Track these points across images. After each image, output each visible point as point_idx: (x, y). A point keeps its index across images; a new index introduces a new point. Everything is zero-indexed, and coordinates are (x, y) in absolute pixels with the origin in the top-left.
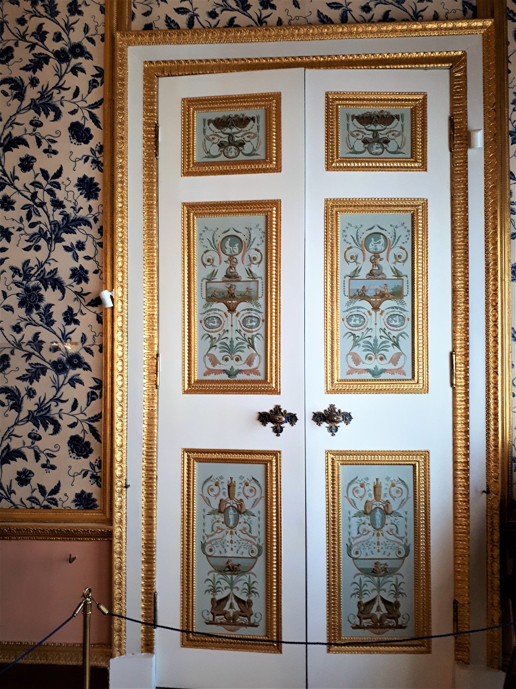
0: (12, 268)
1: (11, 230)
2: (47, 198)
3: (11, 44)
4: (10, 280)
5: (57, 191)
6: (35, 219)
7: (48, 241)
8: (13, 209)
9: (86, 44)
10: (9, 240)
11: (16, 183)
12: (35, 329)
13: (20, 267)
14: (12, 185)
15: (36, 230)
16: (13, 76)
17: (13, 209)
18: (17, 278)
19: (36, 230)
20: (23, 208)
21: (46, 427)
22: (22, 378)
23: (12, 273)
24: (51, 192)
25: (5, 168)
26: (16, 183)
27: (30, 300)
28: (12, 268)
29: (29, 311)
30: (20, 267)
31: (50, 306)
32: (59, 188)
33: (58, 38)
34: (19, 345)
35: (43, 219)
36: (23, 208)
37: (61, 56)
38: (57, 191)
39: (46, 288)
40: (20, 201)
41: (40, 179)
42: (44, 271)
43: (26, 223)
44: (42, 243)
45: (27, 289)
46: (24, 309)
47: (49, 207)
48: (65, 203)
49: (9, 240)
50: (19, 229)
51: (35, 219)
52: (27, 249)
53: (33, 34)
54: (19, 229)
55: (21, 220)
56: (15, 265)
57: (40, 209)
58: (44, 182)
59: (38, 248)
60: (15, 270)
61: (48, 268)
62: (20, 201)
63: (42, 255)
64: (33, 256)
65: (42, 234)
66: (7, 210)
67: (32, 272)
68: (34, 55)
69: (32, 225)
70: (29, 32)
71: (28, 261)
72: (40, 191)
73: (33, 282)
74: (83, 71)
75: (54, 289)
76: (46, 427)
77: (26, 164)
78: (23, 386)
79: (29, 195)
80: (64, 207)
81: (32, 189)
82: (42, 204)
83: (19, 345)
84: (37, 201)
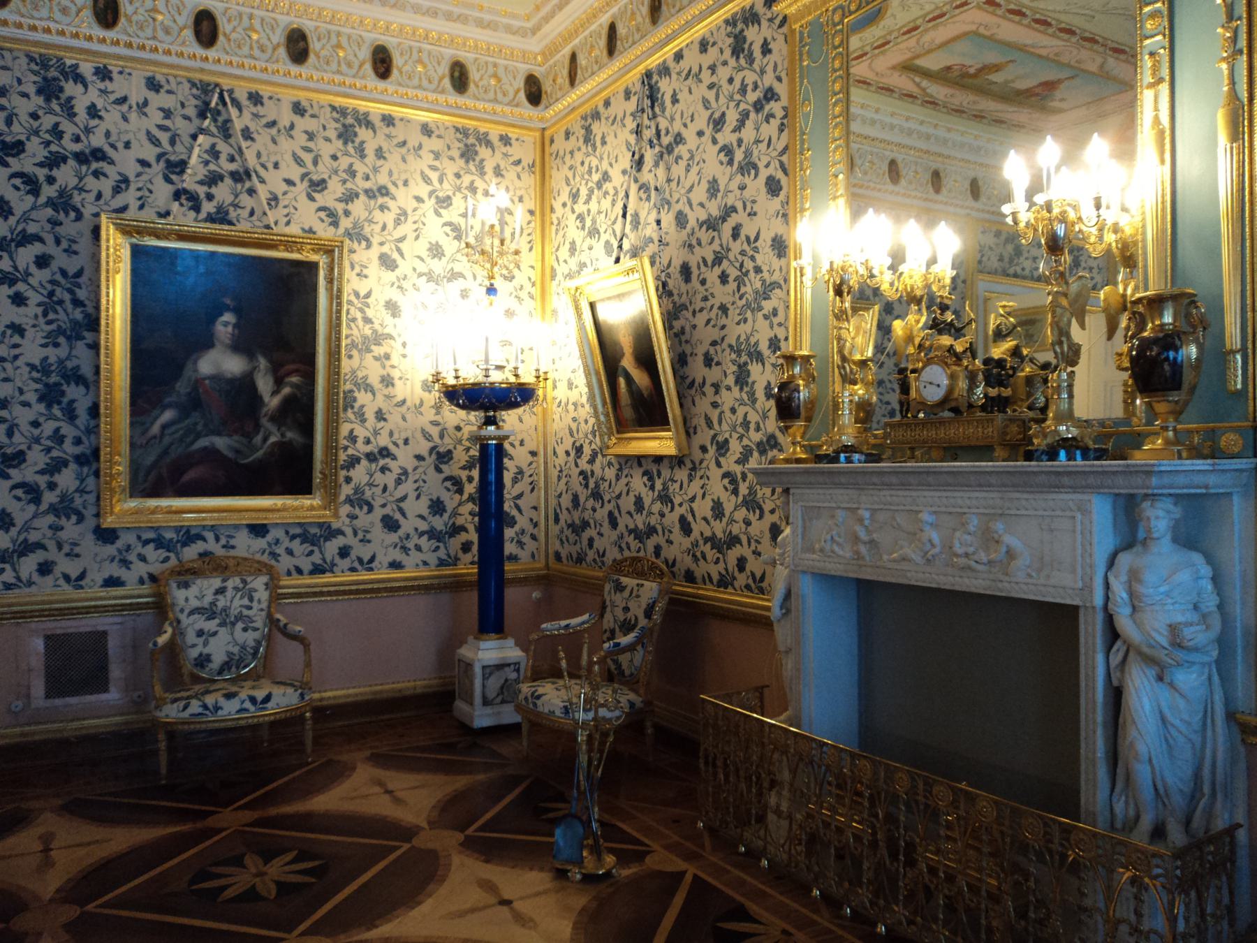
0: (28, 365)
1: (26, 327)
2: (67, 297)
3: (23, 138)
4: (26, 376)
5: (77, 290)
6: (51, 316)
7: (69, 338)
8: (26, 305)
9: (107, 149)
10: (22, 336)
11: (31, 280)
12: (55, 424)
13: (37, 362)
14: (25, 281)
15: (54, 327)
16: (25, 170)
17: (26, 305)
18: (35, 374)
19: (54, 327)
20: (39, 305)
21: (68, 518)
22: (42, 472)
23: (28, 369)
24: (70, 291)
25: (18, 264)
26: (31, 280)
27: (50, 396)
28: (28, 365)
29: (49, 406)
30: (37, 362)
31: (73, 401)
32: (80, 287)
33: (77, 139)
34: (37, 440)
35: (62, 316)
36: (39, 305)
37: (81, 158)
38: (77, 290)
39: (68, 384)
40: (34, 298)
41: (58, 277)
42: (65, 367)
43: (42, 320)
44: (62, 340)
45: (46, 385)
46: (43, 405)
47: (69, 306)
48: (87, 302)
49: (22, 336)
50: (34, 326)
51: (51, 316)
52: (44, 346)
53: (48, 131)
54: (34, 326)
55: (36, 316)
56: (31, 361)
57: (58, 308)
58: (63, 281)
59: (56, 345)
60: (32, 367)
61: (69, 365)
62: (34, 298)
63: (62, 352)
64: (53, 354)
65: (60, 331)
66: (19, 305)
67: (53, 368)
68: (50, 152)
69: (49, 323)
70: (44, 128)
71: (46, 358)
72: (58, 291)
73: (54, 379)
74: (105, 175)
75: (77, 384)
76: (68, 518)
77: (42, 261)
78: (42, 481)
79: (45, 293)
80: (84, 306)
81: (49, 287)
82: (61, 302)
83: (37, 440)
84: (55, 299)
